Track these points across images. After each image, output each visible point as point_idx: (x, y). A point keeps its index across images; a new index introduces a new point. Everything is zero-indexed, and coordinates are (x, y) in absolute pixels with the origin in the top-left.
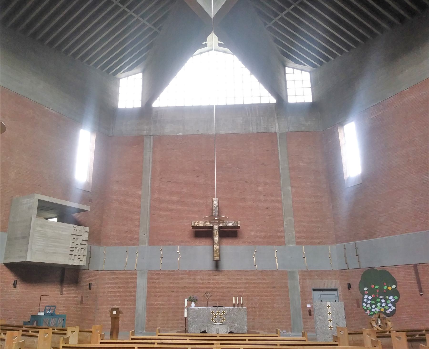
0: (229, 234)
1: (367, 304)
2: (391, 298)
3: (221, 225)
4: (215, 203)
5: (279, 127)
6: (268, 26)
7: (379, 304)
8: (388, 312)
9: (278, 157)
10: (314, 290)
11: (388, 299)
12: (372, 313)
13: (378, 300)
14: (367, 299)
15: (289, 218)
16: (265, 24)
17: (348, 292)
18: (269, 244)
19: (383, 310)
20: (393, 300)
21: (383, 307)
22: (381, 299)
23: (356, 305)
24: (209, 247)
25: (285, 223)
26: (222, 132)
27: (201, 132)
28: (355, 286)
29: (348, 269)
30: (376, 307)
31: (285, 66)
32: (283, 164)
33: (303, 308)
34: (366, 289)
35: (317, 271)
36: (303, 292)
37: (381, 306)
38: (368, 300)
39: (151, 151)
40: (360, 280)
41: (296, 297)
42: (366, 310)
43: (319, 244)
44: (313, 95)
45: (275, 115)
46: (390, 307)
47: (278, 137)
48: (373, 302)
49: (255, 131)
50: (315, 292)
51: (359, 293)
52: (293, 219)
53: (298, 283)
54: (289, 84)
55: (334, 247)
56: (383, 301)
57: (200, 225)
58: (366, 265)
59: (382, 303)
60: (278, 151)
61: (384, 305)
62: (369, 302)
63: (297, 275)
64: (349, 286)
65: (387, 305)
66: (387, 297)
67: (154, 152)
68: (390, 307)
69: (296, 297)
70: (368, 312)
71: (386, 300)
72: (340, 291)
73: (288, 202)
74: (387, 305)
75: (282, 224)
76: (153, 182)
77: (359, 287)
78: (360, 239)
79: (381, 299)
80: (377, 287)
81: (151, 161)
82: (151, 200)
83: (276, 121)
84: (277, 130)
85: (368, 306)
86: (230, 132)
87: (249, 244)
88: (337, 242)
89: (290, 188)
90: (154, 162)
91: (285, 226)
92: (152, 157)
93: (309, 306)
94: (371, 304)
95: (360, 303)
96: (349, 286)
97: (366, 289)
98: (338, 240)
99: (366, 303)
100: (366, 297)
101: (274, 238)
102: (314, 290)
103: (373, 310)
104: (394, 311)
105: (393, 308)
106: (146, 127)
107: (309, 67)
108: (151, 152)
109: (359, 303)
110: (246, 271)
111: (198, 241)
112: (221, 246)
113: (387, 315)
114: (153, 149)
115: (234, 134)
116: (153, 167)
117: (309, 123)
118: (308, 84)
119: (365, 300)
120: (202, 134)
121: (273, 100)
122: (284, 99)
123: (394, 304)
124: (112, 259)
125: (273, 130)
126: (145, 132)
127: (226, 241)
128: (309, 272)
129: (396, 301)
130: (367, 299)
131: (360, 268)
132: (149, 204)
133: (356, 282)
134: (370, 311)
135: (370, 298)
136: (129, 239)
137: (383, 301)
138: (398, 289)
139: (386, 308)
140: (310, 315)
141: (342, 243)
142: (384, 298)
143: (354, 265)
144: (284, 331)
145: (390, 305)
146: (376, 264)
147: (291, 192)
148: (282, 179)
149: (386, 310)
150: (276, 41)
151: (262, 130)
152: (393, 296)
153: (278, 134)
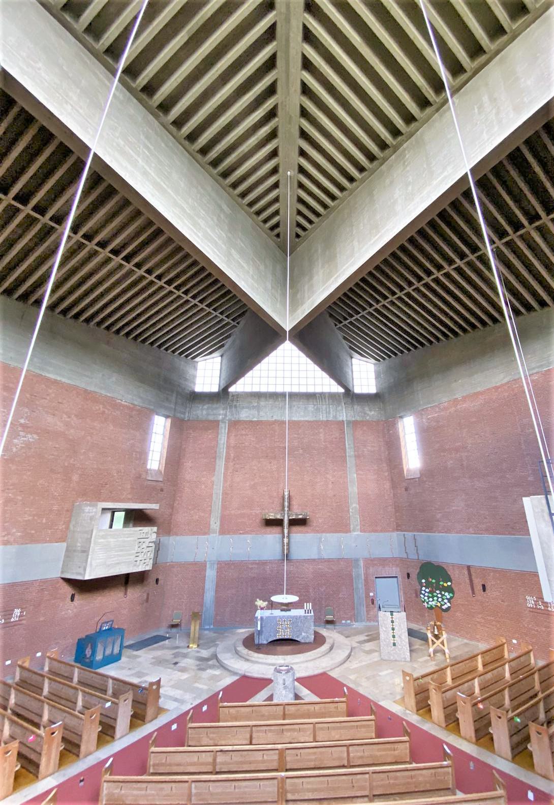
0: (299, 522)
1: (425, 596)
2: (446, 594)
3: (291, 518)
4: (286, 493)
5: (346, 416)
6: (337, 327)
7: (435, 598)
8: (444, 607)
9: (345, 444)
10: (376, 578)
11: (444, 595)
12: (429, 606)
13: (435, 594)
14: (425, 591)
15: (354, 505)
16: (336, 325)
17: (406, 580)
18: (336, 532)
19: (439, 604)
20: (448, 597)
21: (440, 602)
22: (438, 594)
23: (414, 595)
24: (279, 536)
25: (351, 510)
26: (295, 419)
27: (275, 418)
28: (414, 576)
29: (408, 558)
30: (433, 600)
31: (352, 358)
32: (350, 452)
33: (366, 597)
34: (423, 581)
35: (380, 559)
36: (366, 580)
37: (437, 600)
38: (426, 592)
39: (226, 436)
40: (418, 571)
41: (360, 585)
42: (424, 602)
43: (381, 531)
44: (376, 386)
45: (343, 404)
46: (446, 603)
47: (345, 425)
48: (430, 595)
49: (325, 419)
50: (377, 579)
51: (418, 584)
52: (358, 506)
53: (362, 571)
54: (356, 375)
55: (395, 534)
56: (439, 596)
57: (271, 518)
58: (424, 558)
59: (438, 598)
60: (345, 438)
61: (440, 600)
62: (426, 594)
63: (361, 563)
64: (408, 575)
65: (443, 600)
66: (443, 593)
67: (228, 438)
68: (446, 603)
69: (360, 585)
70: (425, 604)
71: (443, 595)
72: (400, 579)
73: (353, 490)
74: (443, 600)
75: (348, 511)
76: (226, 468)
77: (418, 578)
78: (419, 531)
79: (438, 594)
80: (434, 581)
81: (225, 446)
82: (223, 487)
83: (344, 409)
84: (345, 419)
85: (426, 598)
86: (302, 419)
87: (318, 532)
88: (397, 530)
89: (355, 475)
90: (228, 447)
91: (351, 514)
92: (227, 442)
93: (371, 594)
94: (429, 597)
95: (419, 593)
96: (408, 575)
97: (423, 581)
98: (398, 528)
99: (424, 595)
100: (424, 588)
101: (341, 526)
102: (376, 578)
103: (430, 603)
104: (449, 608)
105: (449, 604)
106: (222, 412)
107: (373, 361)
108: (226, 438)
109: (418, 594)
110: (314, 560)
111: (269, 529)
112: (291, 535)
113: (443, 610)
114: (228, 433)
115: (307, 421)
116: (227, 453)
117: (373, 413)
118: (372, 375)
119: (423, 592)
120: (275, 420)
121: (341, 390)
122: (351, 389)
123: (449, 600)
124: (185, 548)
125: (341, 419)
126: (221, 417)
127: (295, 529)
128: (372, 560)
129: (451, 598)
130: (425, 591)
131: (418, 559)
132: (221, 491)
133: (414, 574)
134: (427, 603)
135: (427, 590)
136: (202, 529)
137: (439, 596)
138: (453, 586)
139: (443, 603)
140: (373, 603)
141: (402, 531)
142: (441, 594)
143: (413, 556)
144: (349, 622)
145: (446, 601)
146: (433, 560)
147: (356, 479)
148: (348, 466)
149: (442, 605)
150: (345, 338)
151: (331, 419)
152: (449, 593)
153: (345, 422)
